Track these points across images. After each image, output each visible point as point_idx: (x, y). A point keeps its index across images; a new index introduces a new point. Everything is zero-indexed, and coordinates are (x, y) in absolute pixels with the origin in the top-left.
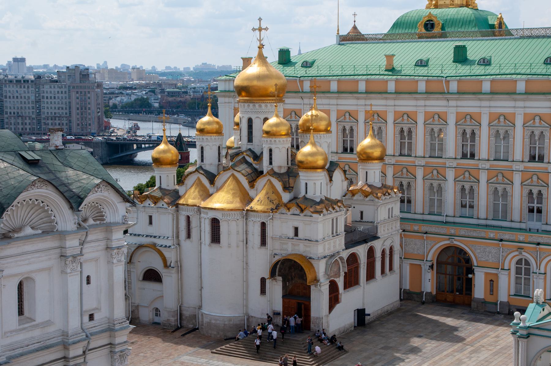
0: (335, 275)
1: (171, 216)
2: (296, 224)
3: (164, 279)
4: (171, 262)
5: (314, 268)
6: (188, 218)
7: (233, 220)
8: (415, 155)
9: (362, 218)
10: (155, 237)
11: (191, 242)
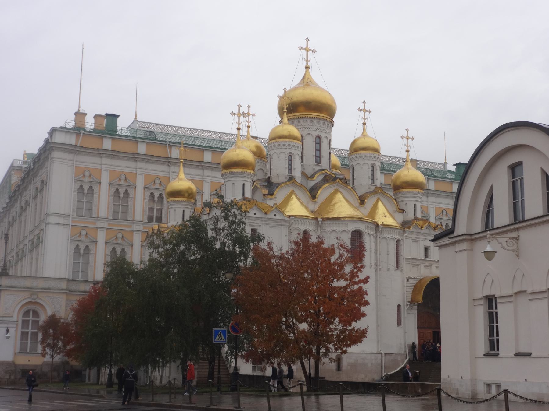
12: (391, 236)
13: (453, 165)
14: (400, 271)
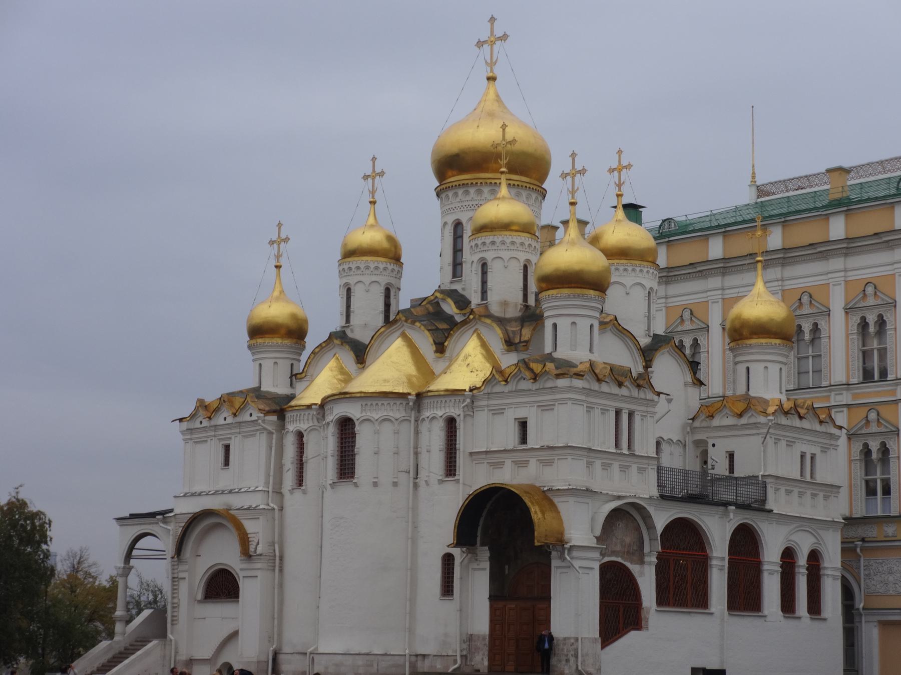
0: (628, 552)
1: (264, 437)
2: (521, 413)
4: (258, 543)
5: (559, 512)
6: (300, 435)
7: (385, 420)
8: (894, 376)
9: (731, 470)
10: (230, 492)
11: (304, 492)
12: (432, 412)
13: (645, 207)
14: (454, 482)
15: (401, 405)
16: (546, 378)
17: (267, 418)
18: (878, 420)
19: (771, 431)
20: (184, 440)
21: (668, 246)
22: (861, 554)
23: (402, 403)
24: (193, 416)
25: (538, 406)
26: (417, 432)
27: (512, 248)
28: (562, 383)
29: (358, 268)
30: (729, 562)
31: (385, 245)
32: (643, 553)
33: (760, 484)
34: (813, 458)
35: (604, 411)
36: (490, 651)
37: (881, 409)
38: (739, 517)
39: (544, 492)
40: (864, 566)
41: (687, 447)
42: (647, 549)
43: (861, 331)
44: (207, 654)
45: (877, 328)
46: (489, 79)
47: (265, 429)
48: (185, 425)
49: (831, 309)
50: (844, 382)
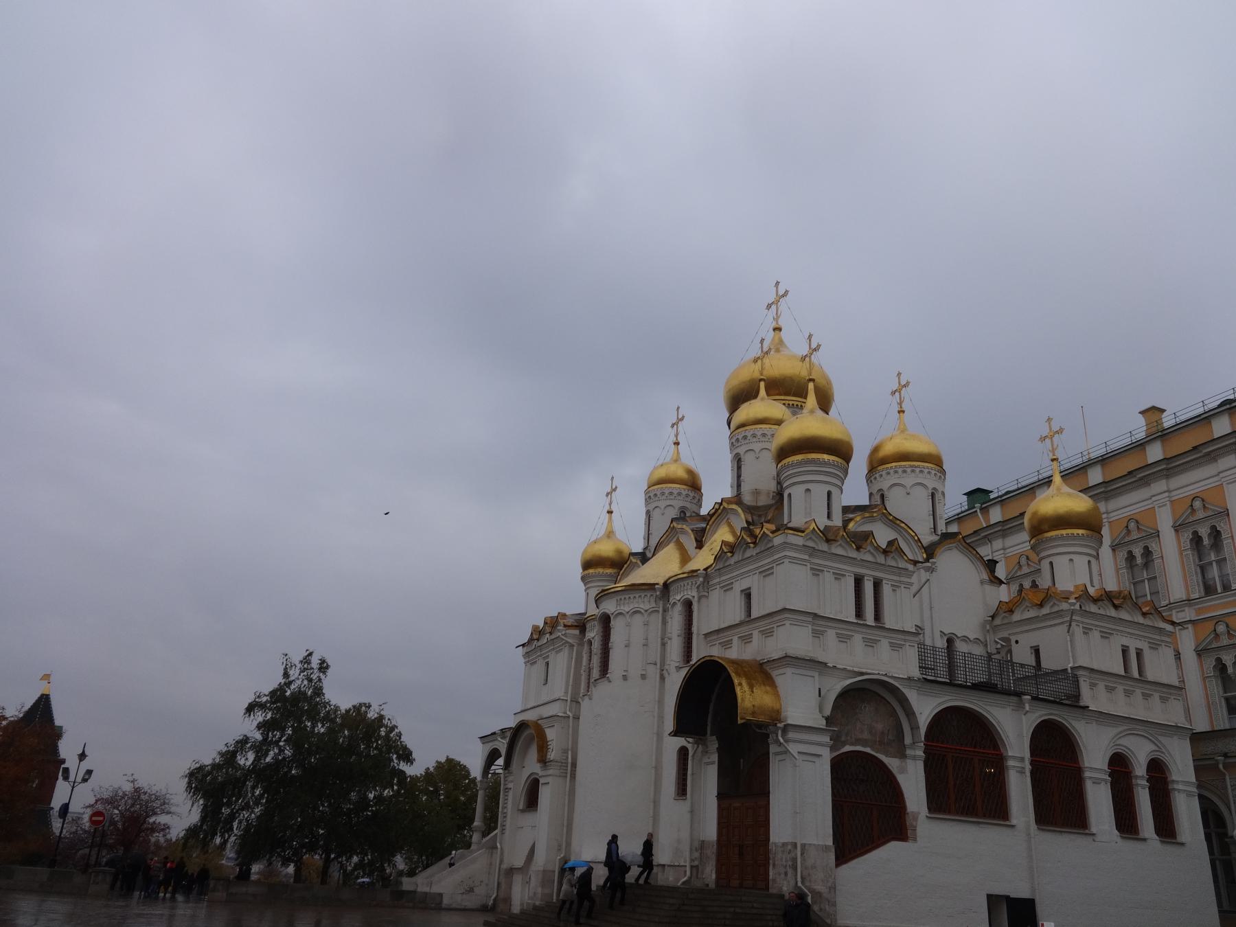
1: (566, 650)
2: (745, 584)
3: (545, 795)
5: (776, 687)
15: (652, 597)
16: (766, 541)
17: (568, 631)
18: (1228, 631)
19: (1074, 618)
20: (525, 663)
21: (1002, 506)
22: (1224, 771)
23: (652, 595)
24: (531, 640)
25: (760, 572)
26: (664, 622)
27: (763, 440)
28: (778, 540)
29: (656, 495)
30: (1031, 764)
31: (681, 473)
32: (904, 745)
33: (1070, 677)
34: (1139, 654)
35: (838, 576)
36: (718, 861)
37: (1227, 620)
38: (1043, 712)
39: (761, 664)
40: (1232, 786)
41: (989, 647)
42: (908, 740)
43: (1195, 547)
44: (519, 862)
45: (1212, 541)
46: (775, 329)
47: (567, 642)
48: (525, 648)
49: (1159, 529)
50: (1184, 599)
